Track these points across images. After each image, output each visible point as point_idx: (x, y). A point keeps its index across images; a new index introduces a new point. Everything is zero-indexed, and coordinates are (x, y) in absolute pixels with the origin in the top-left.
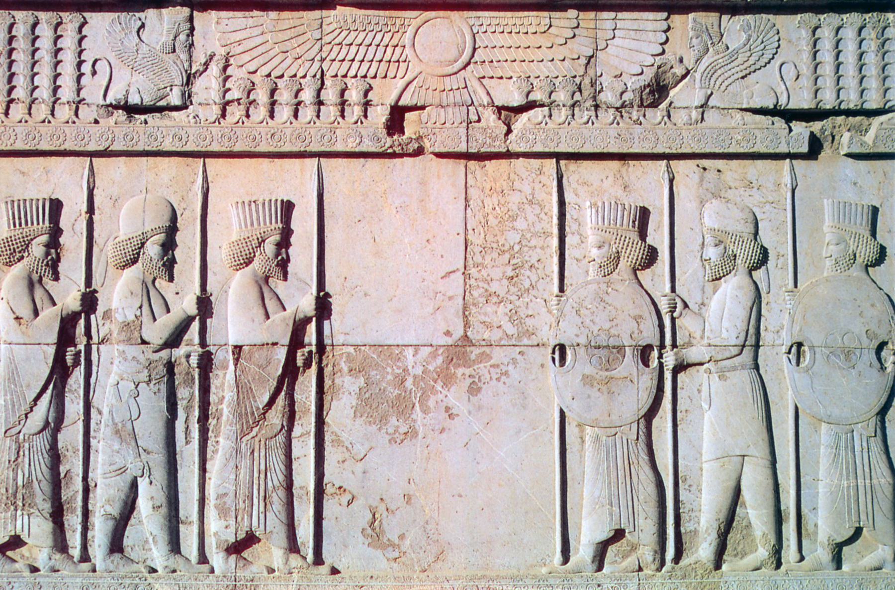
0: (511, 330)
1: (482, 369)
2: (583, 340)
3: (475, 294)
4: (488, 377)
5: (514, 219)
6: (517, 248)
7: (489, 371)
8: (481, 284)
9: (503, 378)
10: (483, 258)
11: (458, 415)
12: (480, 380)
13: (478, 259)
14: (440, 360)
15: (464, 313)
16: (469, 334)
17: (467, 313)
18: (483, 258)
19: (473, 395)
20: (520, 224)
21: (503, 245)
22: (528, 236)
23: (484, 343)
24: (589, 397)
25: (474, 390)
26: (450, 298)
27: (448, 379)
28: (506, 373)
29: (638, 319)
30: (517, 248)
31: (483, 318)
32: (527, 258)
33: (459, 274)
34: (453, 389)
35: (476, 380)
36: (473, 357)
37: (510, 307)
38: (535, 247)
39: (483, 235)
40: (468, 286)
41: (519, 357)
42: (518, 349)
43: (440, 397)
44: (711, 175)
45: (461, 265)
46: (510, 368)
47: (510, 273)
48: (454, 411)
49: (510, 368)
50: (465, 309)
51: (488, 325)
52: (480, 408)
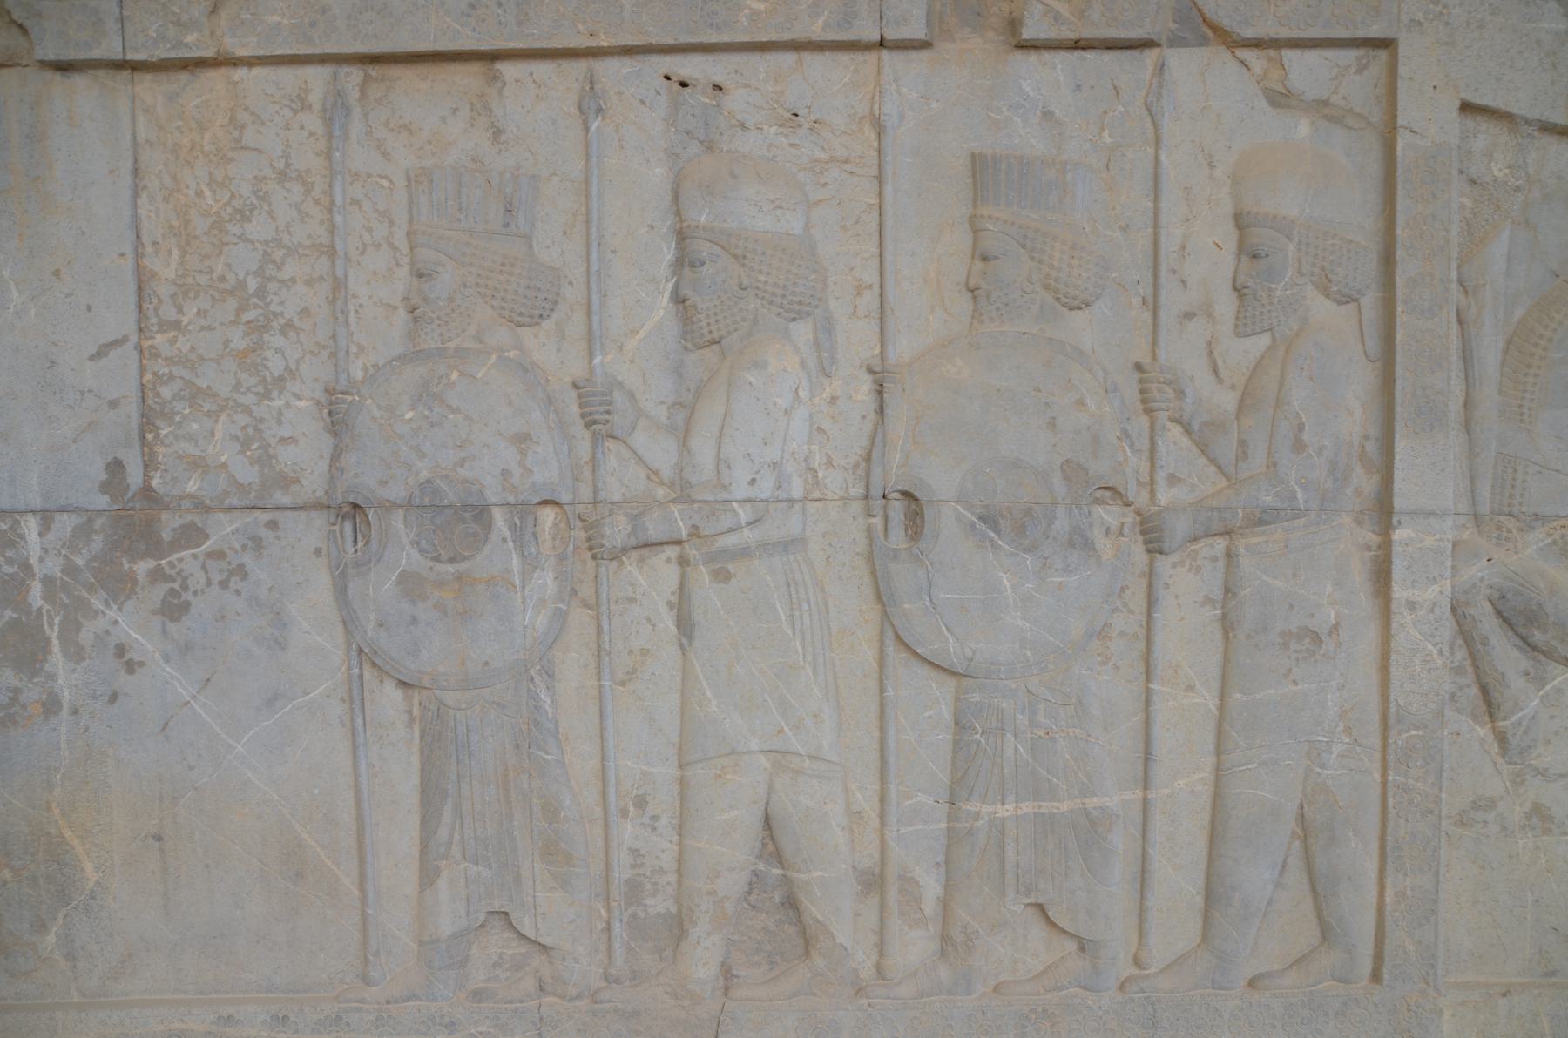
0: (247, 474)
1: (187, 560)
2: (396, 492)
3: (166, 392)
4: (201, 577)
5: (243, 216)
6: (252, 284)
7: (204, 567)
8: (178, 371)
9: (235, 583)
10: (180, 310)
11: (142, 664)
12: (185, 587)
13: (168, 312)
14: (97, 543)
15: (143, 437)
16: (155, 483)
17: (150, 436)
18: (180, 310)
19: (173, 619)
20: (259, 228)
21: (222, 279)
22: (278, 254)
23: (187, 504)
24: (414, 620)
25: (174, 609)
26: (113, 404)
27: (119, 587)
28: (241, 571)
29: (522, 440)
30: (252, 284)
31: (188, 448)
32: (274, 307)
33: (129, 347)
34: (129, 605)
35: (176, 586)
36: (166, 535)
37: (242, 419)
38: (293, 280)
39: (176, 252)
40: (148, 377)
41: (264, 533)
42: (265, 517)
43: (101, 624)
44: (698, 98)
45: (130, 327)
46: (248, 559)
47: (239, 342)
48: (132, 655)
49: (248, 559)
50: (147, 421)
51: (197, 464)
52: (187, 648)
